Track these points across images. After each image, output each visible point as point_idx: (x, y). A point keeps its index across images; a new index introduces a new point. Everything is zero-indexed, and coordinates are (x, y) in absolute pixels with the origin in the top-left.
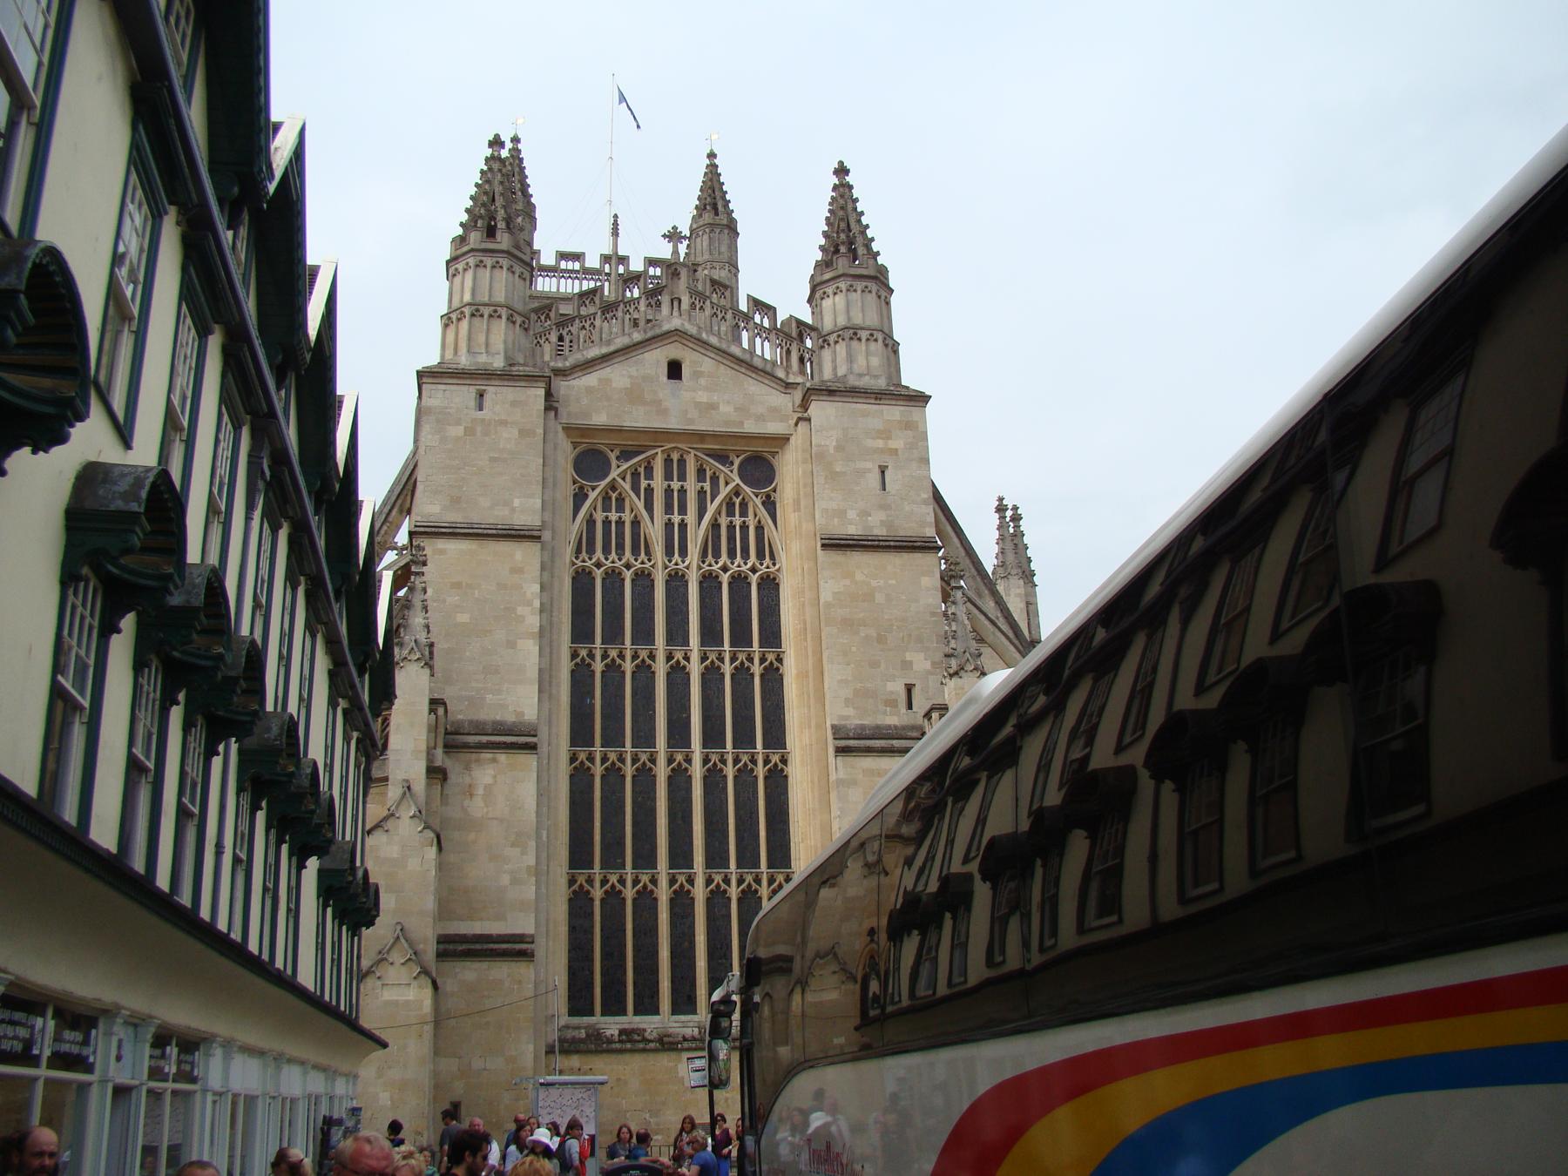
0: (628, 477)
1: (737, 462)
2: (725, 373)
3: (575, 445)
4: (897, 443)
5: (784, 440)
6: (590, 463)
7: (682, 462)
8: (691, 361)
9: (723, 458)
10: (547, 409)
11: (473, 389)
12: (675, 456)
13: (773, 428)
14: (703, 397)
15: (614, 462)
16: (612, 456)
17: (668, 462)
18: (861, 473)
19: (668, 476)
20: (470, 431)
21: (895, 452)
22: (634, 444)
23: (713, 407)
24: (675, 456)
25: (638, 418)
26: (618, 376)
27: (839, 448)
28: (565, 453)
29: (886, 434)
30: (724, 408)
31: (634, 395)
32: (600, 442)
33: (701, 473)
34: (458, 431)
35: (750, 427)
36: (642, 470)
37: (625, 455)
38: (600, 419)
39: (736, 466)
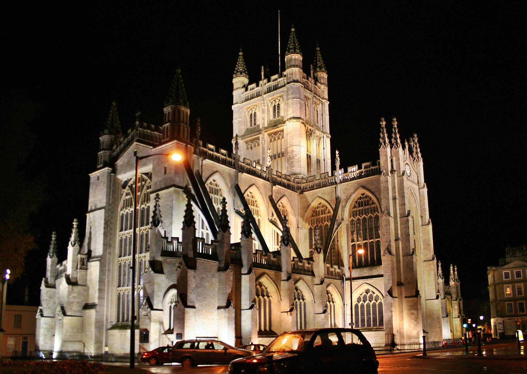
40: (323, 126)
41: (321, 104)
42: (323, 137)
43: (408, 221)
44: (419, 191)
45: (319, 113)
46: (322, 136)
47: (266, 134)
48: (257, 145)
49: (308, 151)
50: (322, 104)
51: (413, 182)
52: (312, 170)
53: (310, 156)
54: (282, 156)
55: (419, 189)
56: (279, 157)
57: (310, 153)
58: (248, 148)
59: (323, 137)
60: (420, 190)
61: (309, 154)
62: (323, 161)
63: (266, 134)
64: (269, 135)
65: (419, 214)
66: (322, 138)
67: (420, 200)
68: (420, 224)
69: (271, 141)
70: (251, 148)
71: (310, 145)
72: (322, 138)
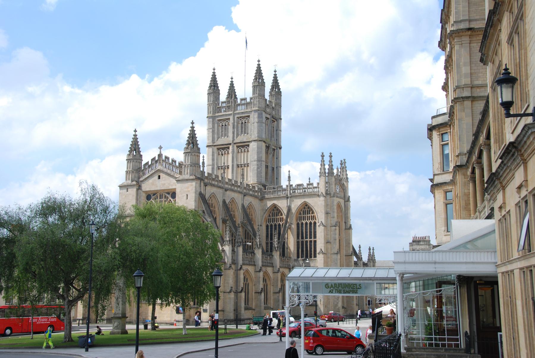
0: (154, 199)
1: (171, 194)
2: (167, 177)
3: (146, 194)
4: (190, 189)
5: (175, 189)
6: (148, 197)
7: (162, 195)
8: (162, 175)
9: (168, 193)
10: (138, 190)
11: (126, 188)
12: (161, 194)
13: (174, 187)
14: (163, 182)
15: (152, 196)
16: (152, 195)
17: (160, 195)
18: (183, 196)
19: (160, 198)
20: (126, 196)
21: (189, 191)
22: (155, 193)
23: (165, 184)
24: (161, 194)
25: (153, 188)
26: (151, 181)
27: (180, 192)
28: (143, 196)
29: (188, 188)
30: (167, 184)
31: (153, 184)
32: (150, 193)
33: (165, 196)
34: (124, 197)
35: (171, 187)
36: (156, 197)
37: (154, 195)
38: (148, 189)
39: (170, 195)
40: (277, 140)
41: (276, 122)
42: (277, 149)
43: (335, 229)
44: (345, 204)
45: (274, 128)
46: (276, 148)
47: (235, 146)
48: (226, 153)
49: (266, 163)
50: (277, 121)
51: (340, 198)
52: (268, 177)
53: (267, 166)
54: (247, 166)
55: (345, 202)
56: (245, 166)
57: (268, 163)
58: (219, 154)
59: (277, 149)
60: (346, 203)
61: (267, 164)
62: (276, 169)
63: (235, 146)
64: (238, 147)
65: (344, 221)
66: (276, 150)
67: (345, 209)
68: (344, 227)
69: (238, 152)
70: (222, 155)
71: (268, 157)
72: (276, 150)
